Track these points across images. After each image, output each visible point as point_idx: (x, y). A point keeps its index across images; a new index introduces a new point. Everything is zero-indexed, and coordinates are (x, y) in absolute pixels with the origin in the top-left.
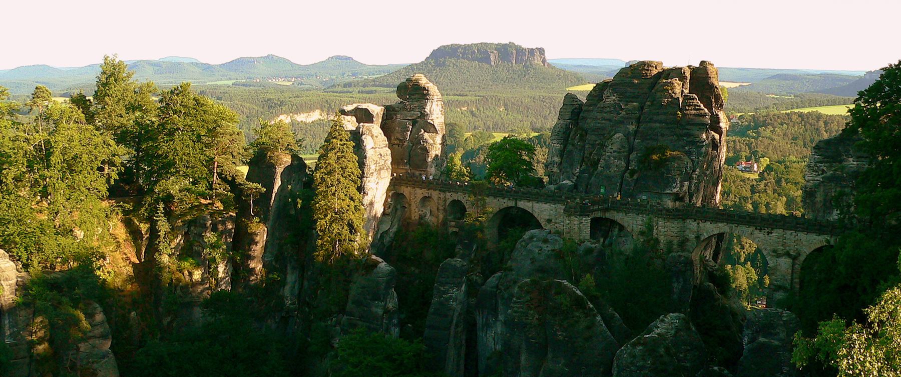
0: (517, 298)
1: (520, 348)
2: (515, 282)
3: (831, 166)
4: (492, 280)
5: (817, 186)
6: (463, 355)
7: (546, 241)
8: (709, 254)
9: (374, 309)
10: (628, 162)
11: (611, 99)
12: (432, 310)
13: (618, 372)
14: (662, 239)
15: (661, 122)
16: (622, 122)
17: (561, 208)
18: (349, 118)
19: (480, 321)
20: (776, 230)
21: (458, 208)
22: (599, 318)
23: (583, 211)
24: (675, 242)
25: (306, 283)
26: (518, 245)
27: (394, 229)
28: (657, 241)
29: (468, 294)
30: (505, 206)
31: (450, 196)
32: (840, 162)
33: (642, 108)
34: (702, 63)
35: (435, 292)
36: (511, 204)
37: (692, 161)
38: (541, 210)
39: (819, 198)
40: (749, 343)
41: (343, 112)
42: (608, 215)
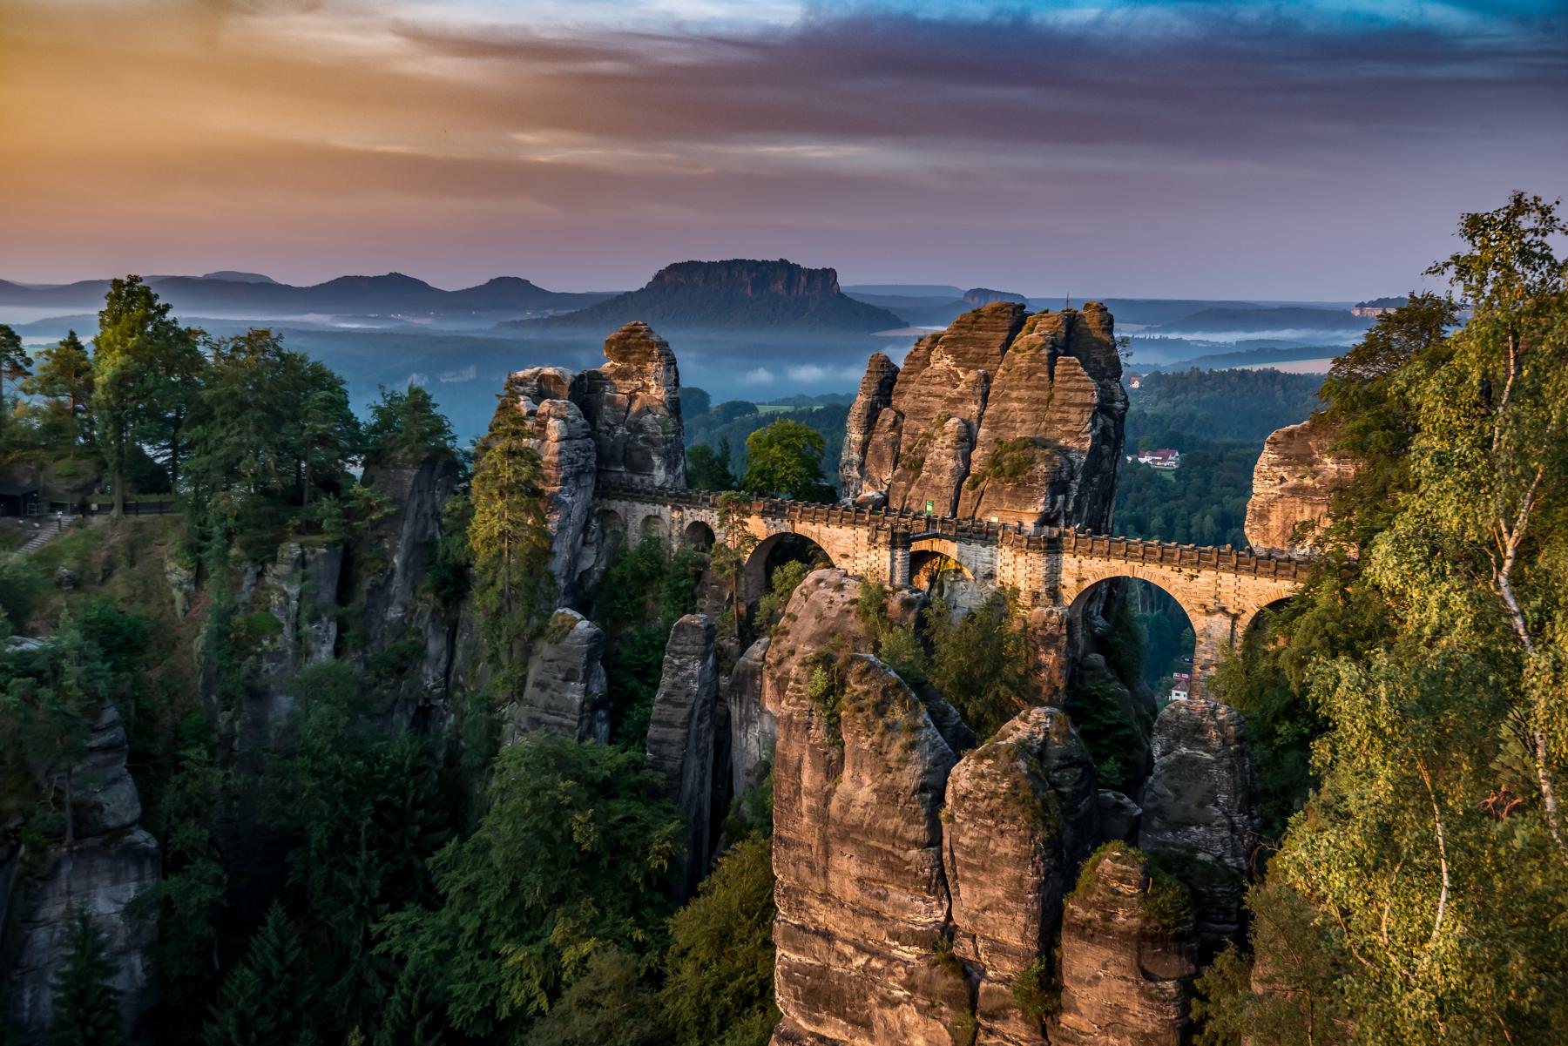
0: (797, 681)
1: (801, 761)
2: (792, 652)
3: (1295, 471)
4: (756, 650)
5: (1271, 503)
6: (709, 767)
7: (840, 587)
8: (1095, 608)
9: (569, 695)
11: (942, 362)
12: (659, 696)
13: (955, 800)
14: (1022, 585)
15: (1019, 400)
16: (962, 401)
17: (863, 533)
18: (527, 389)
19: (736, 711)
20: (1204, 572)
21: (703, 533)
24: (1042, 590)
25: (459, 654)
26: (796, 594)
28: (1016, 591)
29: (717, 670)
30: (773, 532)
31: (692, 515)
32: (1310, 465)
34: (1087, 306)
35: (665, 667)
37: (1071, 461)
38: (836, 538)
39: (1275, 521)
40: (1163, 754)
41: (522, 382)
42: (938, 546)
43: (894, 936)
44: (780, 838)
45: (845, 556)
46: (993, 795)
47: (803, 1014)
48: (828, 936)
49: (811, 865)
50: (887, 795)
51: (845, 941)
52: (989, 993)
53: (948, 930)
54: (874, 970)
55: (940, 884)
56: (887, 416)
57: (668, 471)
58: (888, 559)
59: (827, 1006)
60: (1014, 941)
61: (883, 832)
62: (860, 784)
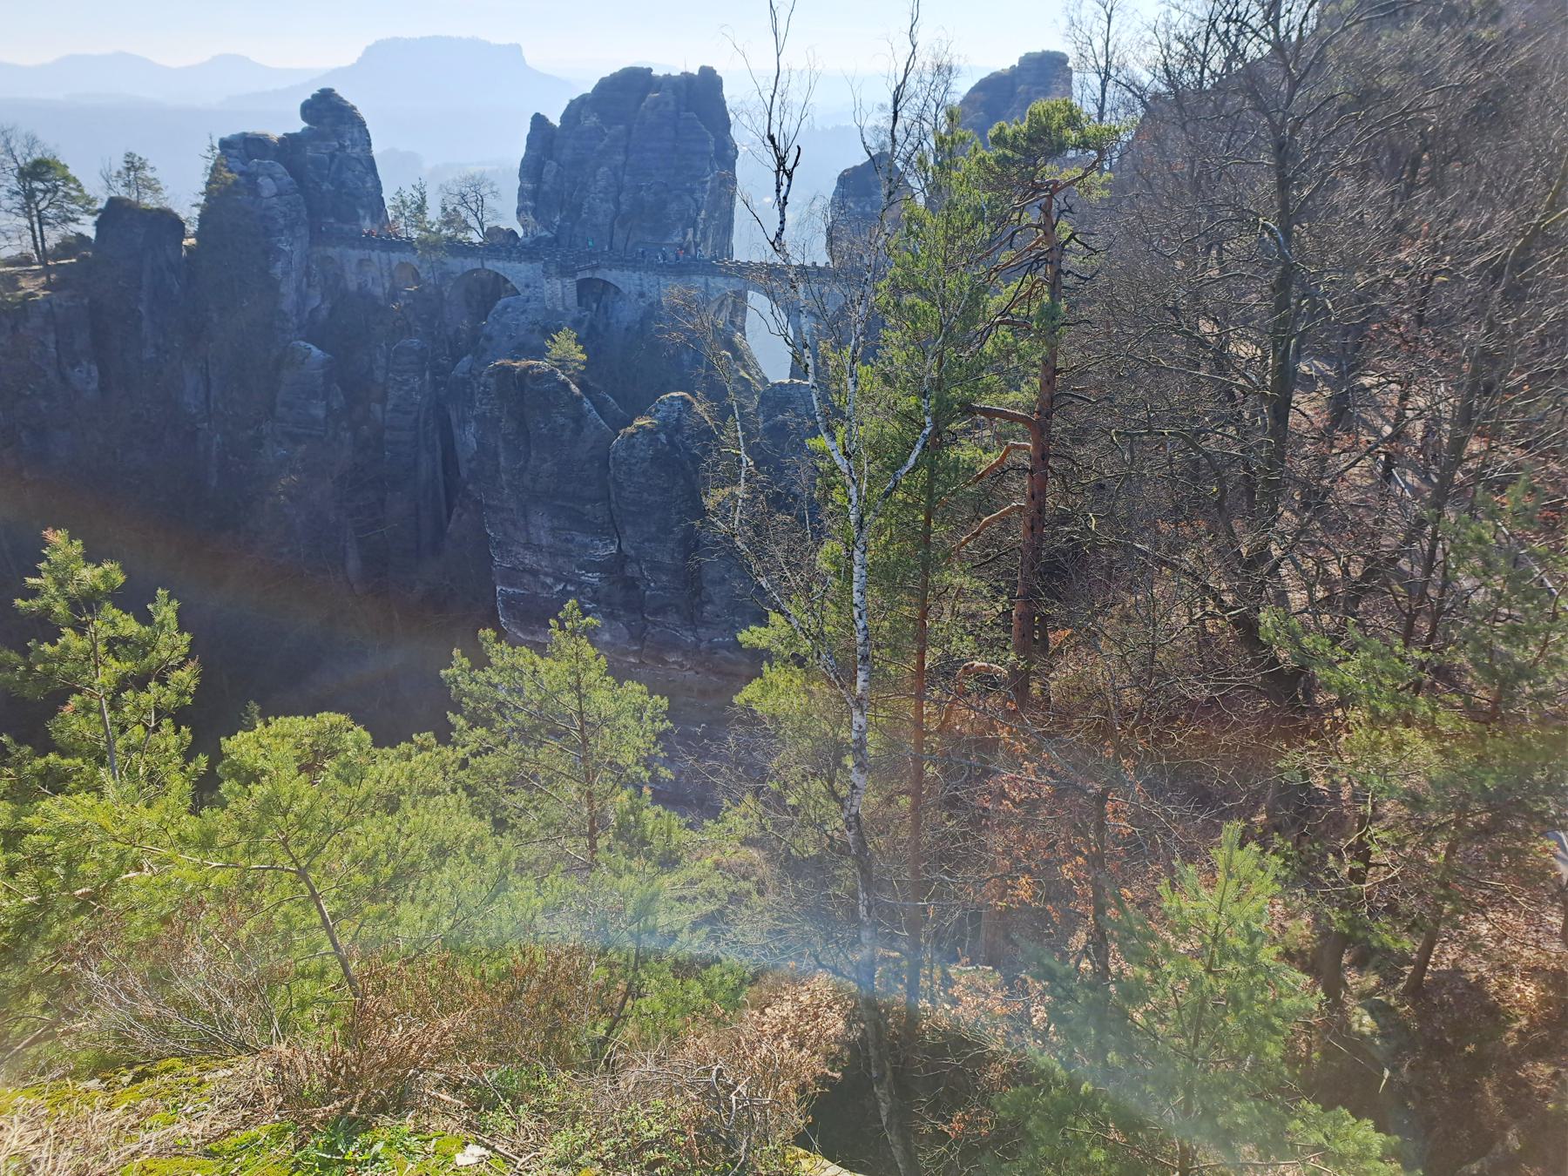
10: (618, 204)
11: (592, 120)
12: (389, 407)
22: (587, 405)
23: (565, 271)
27: (327, 305)
33: (629, 132)
36: (477, 265)
37: (696, 201)
38: (516, 271)
42: (598, 275)
44: (488, 506)
45: (527, 286)
47: (521, 629)
48: (534, 573)
49: (514, 524)
51: (546, 574)
52: (652, 597)
53: (621, 558)
55: (612, 529)
56: (551, 166)
57: (373, 221)
58: (559, 286)
60: (667, 560)
62: (545, 461)
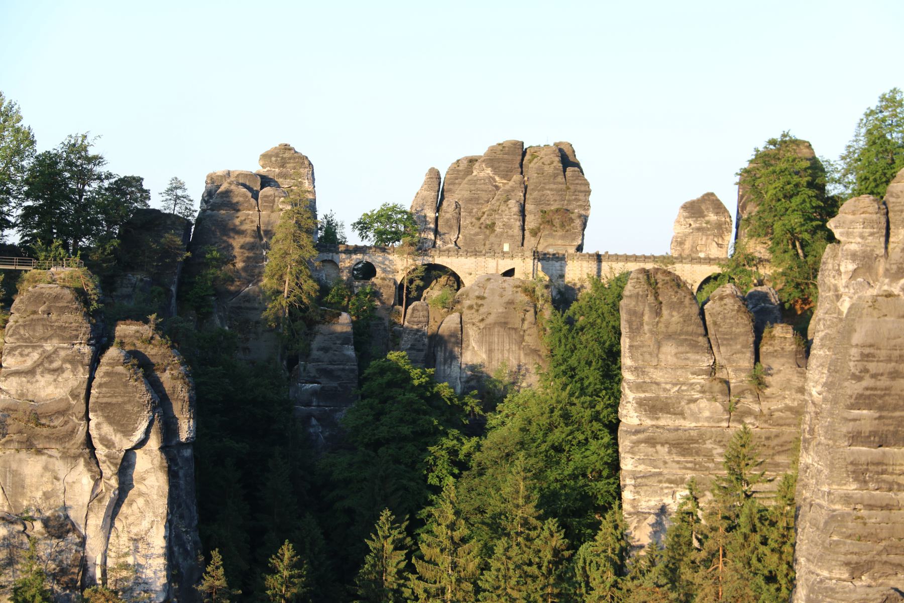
43: (693, 374)
46: (733, 310)
50: (686, 319)
54: (683, 391)
59: (661, 410)
61: (687, 333)
